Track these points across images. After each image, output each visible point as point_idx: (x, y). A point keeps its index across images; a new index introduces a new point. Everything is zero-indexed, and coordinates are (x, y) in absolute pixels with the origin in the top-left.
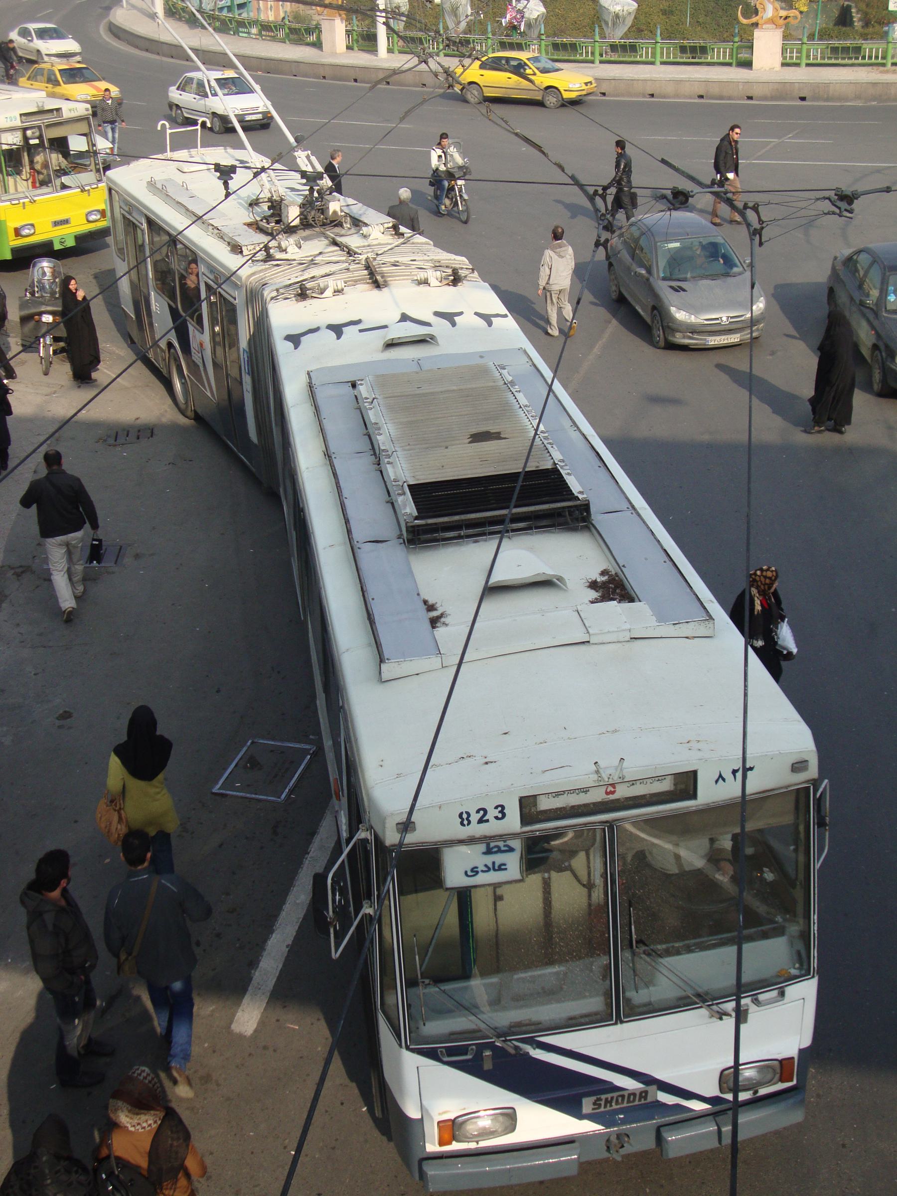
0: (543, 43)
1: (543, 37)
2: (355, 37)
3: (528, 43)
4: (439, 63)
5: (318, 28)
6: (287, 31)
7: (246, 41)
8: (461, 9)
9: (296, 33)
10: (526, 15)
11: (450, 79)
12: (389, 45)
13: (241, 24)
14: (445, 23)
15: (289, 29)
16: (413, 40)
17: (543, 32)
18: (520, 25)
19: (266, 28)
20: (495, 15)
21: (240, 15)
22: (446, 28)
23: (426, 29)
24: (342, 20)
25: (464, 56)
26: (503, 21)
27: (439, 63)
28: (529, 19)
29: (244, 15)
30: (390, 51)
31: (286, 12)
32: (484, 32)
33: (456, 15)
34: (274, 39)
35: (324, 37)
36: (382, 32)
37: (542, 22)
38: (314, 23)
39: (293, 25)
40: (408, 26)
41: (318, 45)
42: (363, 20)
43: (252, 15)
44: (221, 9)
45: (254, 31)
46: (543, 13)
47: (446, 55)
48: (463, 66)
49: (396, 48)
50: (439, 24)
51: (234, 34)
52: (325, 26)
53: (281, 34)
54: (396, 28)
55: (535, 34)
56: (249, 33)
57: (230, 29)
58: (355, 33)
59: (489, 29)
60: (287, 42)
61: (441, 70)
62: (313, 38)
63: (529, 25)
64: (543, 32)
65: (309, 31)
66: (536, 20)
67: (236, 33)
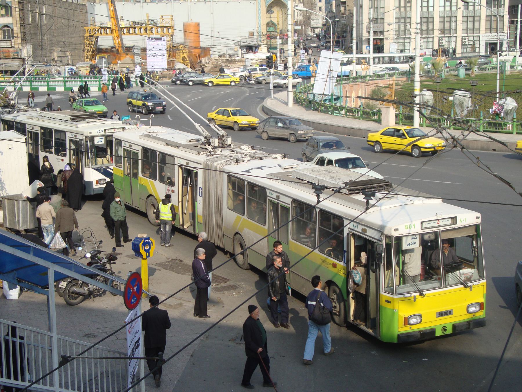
0: (515, 123)
1: (515, 120)
2: (401, 117)
3: (505, 123)
4: (449, 133)
5: (379, 112)
6: (362, 113)
7: (338, 118)
8: (465, 103)
9: (367, 115)
10: (505, 107)
11: (455, 142)
12: (420, 122)
13: (336, 109)
14: (455, 111)
15: (363, 112)
16: (435, 120)
17: (515, 117)
18: (501, 113)
19: (349, 111)
20: (486, 107)
21: (335, 104)
22: (455, 114)
23: (443, 114)
24: (394, 108)
25: (464, 130)
26: (490, 110)
27: (449, 133)
28: (507, 110)
29: (338, 104)
30: (421, 125)
31: (361, 103)
32: (478, 117)
33: (461, 107)
34: (354, 117)
35: (382, 117)
36: (417, 115)
37: (514, 112)
38: (378, 109)
39: (365, 110)
40: (432, 112)
41: (379, 121)
42: (406, 108)
43: (342, 104)
44: (325, 100)
45: (343, 112)
46: (516, 107)
47: (454, 129)
48: (463, 135)
49: (424, 124)
50: (451, 111)
51: (331, 114)
52: (383, 111)
53: (358, 115)
54: (425, 114)
55: (510, 118)
56: (339, 114)
57: (329, 112)
58: (401, 115)
59: (482, 114)
60: (361, 119)
61: (449, 137)
62: (376, 117)
63: (507, 113)
64: (515, 117)
65: (374, 114)
66: (511, 110)
67: (332, 113)
